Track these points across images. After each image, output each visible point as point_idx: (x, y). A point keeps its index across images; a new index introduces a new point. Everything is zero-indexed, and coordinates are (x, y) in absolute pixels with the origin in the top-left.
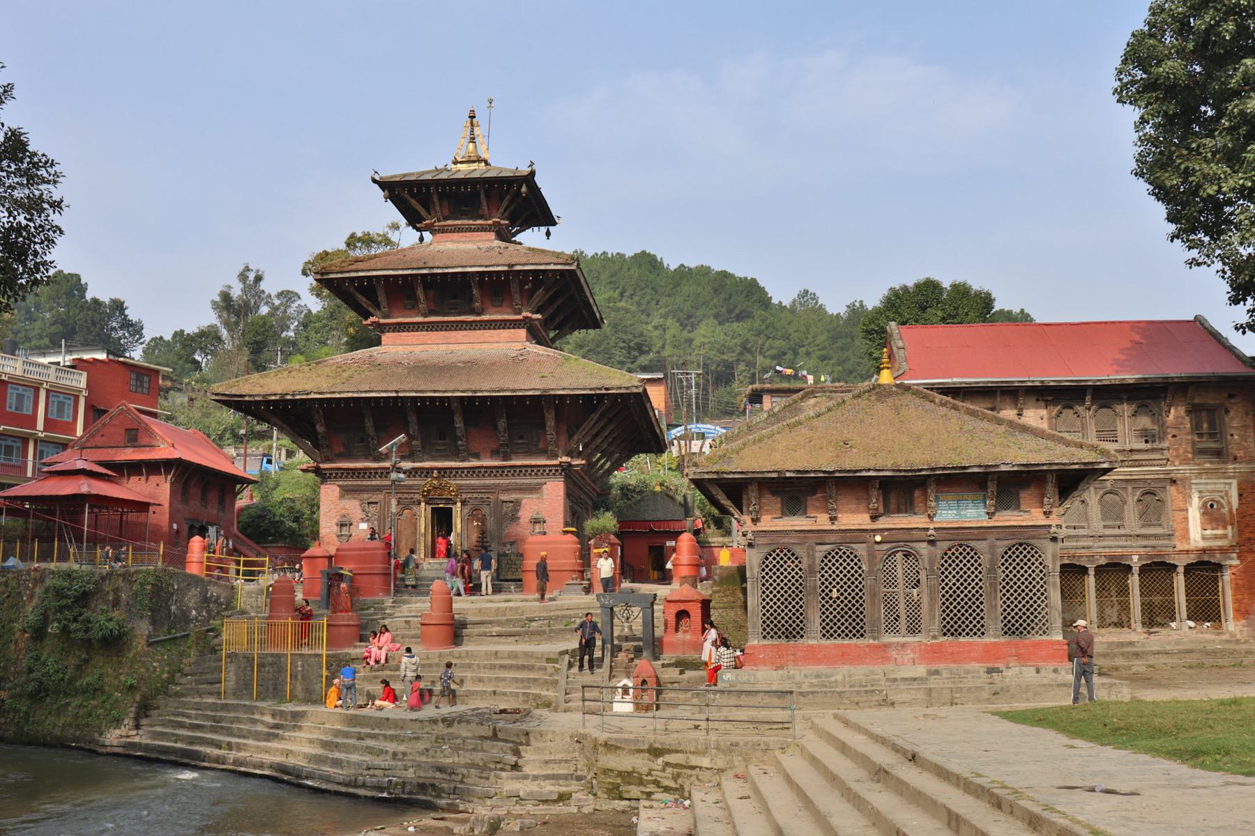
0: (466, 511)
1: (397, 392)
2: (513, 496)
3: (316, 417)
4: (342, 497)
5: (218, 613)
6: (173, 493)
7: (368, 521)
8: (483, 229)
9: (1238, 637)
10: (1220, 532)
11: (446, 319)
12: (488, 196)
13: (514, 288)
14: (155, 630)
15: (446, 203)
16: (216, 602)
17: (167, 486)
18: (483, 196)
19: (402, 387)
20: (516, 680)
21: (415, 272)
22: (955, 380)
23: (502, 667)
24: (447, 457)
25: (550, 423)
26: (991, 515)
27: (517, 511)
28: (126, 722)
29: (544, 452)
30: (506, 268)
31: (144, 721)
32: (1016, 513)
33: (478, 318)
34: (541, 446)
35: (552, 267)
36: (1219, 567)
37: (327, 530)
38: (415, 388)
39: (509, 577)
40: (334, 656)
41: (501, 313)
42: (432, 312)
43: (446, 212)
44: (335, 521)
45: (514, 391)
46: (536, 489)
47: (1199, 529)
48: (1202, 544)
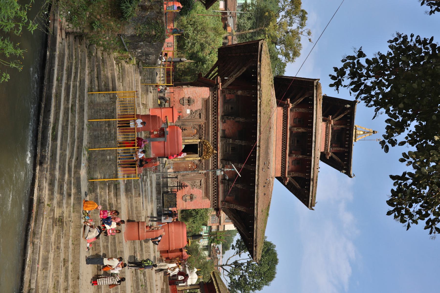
1: (259, 146)
2: (203, 185)
4: (203, 99)
5: (140, 60)
7: (191, 113)
11: (288, 140)
14: (128, 37)
16: (146, 58)
19: (261, 149)
21: (314, 134)
28: (71, 26)
30: (312, 177)
31: (72, 38)
33: (287, 156)
37: (186, 92)
38: (261, 155)
39: (164, 198)
44: (191, 97)
45: (257, 204)
46: (207, 195)
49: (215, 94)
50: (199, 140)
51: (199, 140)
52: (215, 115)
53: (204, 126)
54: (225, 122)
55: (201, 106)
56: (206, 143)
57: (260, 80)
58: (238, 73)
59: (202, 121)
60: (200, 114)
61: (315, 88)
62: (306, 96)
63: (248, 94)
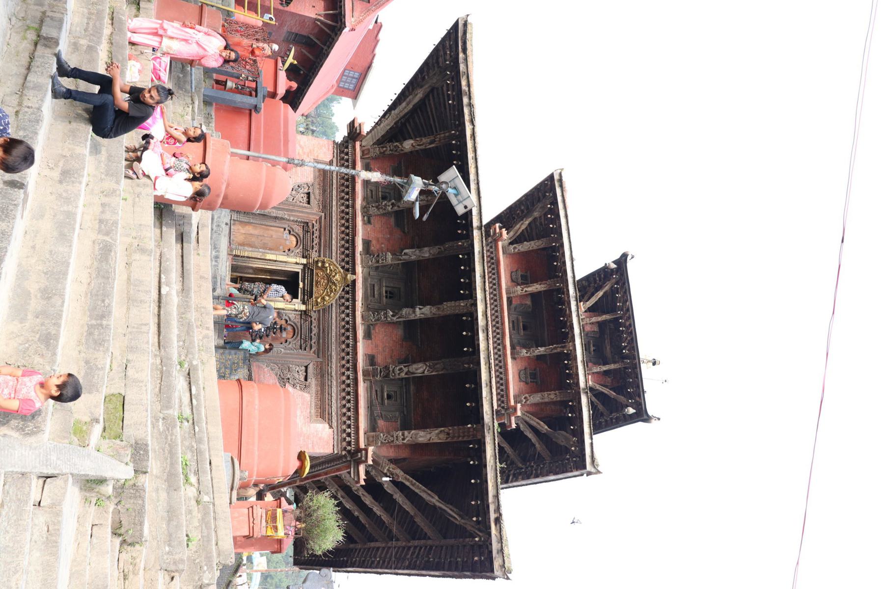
0: (292, 316)
2: (313, 381)
3: (424, 140)
6: (303, 19)
12: (606, 373)
13: (551, 396)
15: (596, 329)
17: (313, 16)
18: (612, 366)
20: (57, 273)
23: (105, 252)
24: (365, 297)
25: (423, 436)
27: (294, 386)
29: (373, 427)
34: (381, 423)
42: (509, 300)
49: (347, 154)
50: (304, 261)
51: (304, 261)
52: (348, 200)
53: (317, 226)
54: (369, 222)
55: (312, 176)
56: (323, 262)
57: (469, 85)
58: (404, 104)
59: (313, 213)
60: (308, 194)
61: (557, 184)
62: (536, 214)
63: (431, 143)
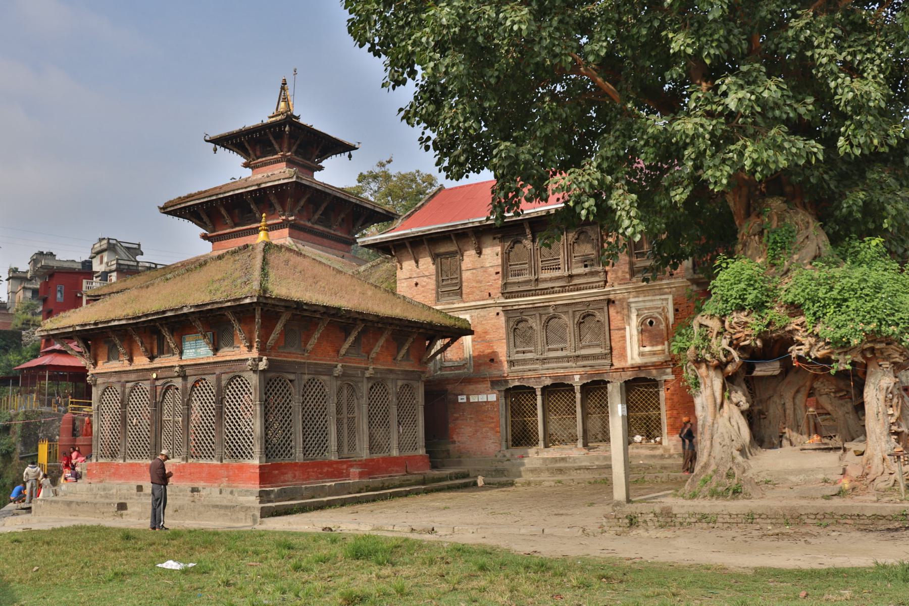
8: (277, 161)
9: (672, 451)
10: (659, 348)
14: (26, 449)
15: (258, 147)
22: (414, 230)
26: (216, 350)
30: (256, 188)
32: (231, 349)
35: (282, 182)
36: (654, 384)
40: (53, 466)
41: (273, 219)
42: (236, 225)
43: (258, 153)
47: (636, 347)
48: (638, 361)
